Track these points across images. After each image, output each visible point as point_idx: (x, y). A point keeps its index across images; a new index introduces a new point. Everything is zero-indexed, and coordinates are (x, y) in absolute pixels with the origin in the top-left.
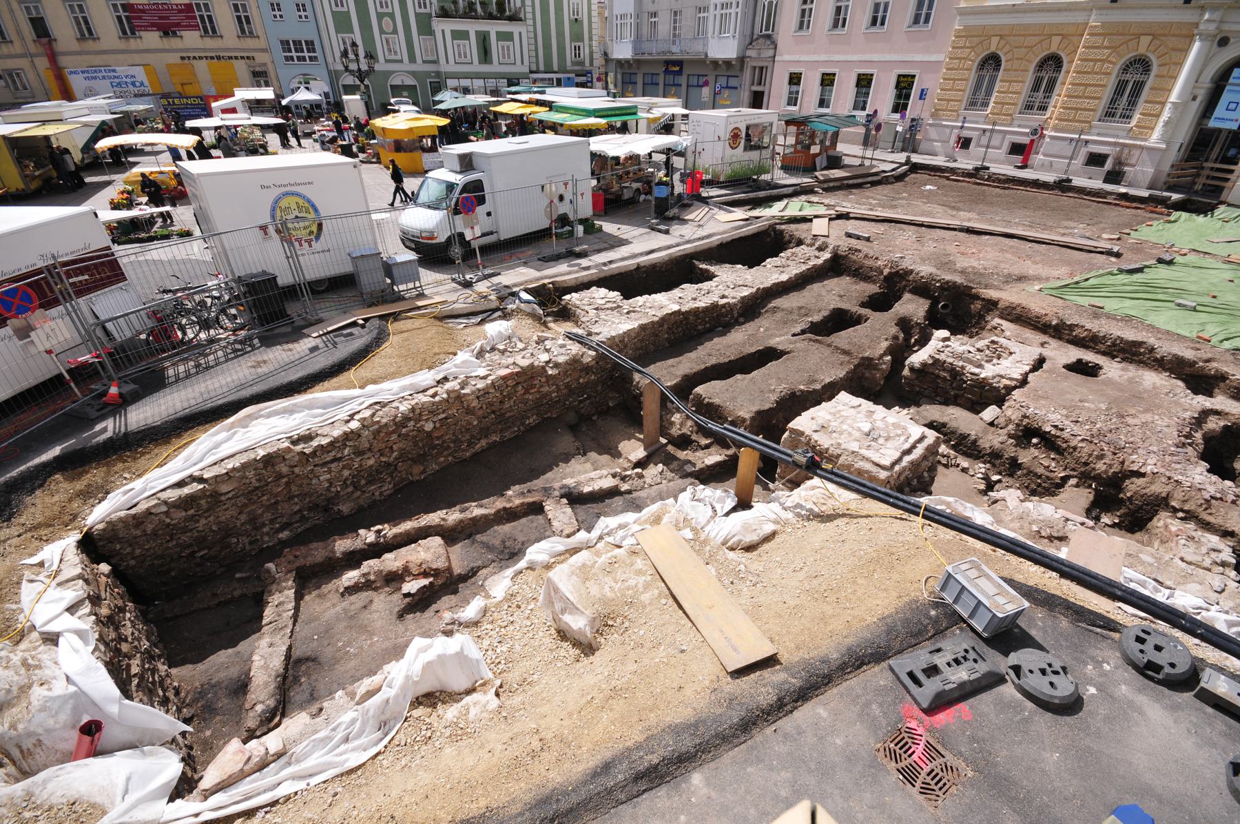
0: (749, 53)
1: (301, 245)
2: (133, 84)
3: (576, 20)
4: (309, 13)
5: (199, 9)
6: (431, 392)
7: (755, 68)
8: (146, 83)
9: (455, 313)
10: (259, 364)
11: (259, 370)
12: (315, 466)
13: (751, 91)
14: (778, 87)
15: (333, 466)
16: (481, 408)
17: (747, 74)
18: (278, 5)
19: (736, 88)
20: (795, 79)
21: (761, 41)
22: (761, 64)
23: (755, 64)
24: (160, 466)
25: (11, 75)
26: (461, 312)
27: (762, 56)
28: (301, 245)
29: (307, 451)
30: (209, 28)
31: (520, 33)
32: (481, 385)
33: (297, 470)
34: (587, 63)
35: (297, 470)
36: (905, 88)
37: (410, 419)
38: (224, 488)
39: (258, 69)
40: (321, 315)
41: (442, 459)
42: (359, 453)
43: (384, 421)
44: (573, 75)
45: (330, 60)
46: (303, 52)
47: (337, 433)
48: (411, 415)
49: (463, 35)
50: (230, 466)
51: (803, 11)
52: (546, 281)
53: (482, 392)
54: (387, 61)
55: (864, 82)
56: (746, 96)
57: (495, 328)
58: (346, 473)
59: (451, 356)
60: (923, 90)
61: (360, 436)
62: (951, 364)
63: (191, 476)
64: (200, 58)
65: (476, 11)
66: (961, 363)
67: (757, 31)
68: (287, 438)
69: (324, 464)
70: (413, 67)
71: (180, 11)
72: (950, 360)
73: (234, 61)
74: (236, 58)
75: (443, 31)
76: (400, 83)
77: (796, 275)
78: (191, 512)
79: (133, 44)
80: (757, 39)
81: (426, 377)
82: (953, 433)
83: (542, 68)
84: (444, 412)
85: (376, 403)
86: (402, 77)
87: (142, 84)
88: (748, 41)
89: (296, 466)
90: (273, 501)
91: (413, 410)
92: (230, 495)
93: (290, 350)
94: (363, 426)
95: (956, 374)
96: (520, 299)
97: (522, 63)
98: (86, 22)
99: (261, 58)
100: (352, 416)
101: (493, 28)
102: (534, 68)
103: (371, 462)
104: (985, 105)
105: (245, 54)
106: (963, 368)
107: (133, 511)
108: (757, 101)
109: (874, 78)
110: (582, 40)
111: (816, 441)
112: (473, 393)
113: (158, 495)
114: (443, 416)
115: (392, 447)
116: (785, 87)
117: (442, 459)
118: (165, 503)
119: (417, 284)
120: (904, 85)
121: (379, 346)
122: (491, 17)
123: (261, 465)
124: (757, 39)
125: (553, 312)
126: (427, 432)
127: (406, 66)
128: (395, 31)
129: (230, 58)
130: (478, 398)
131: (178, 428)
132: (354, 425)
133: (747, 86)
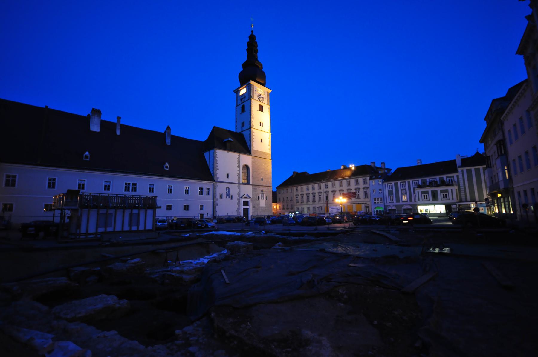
4: (382, 191)
18: (375, 190)
25: (320, 208)
30: (358, 197)
39: (367, 206)
45: (385, 203)
46: (376, 201)
54: (389, 203)
64: (355, 204)
70: (411, 203)
71: (353, 193)
73: (362, 204)
74: (362, 203)
76: (406, 208)
86: (407, 206)
99: (368, 203)
105: (364, 202)
127: (409, 203)
129: (361, 203)
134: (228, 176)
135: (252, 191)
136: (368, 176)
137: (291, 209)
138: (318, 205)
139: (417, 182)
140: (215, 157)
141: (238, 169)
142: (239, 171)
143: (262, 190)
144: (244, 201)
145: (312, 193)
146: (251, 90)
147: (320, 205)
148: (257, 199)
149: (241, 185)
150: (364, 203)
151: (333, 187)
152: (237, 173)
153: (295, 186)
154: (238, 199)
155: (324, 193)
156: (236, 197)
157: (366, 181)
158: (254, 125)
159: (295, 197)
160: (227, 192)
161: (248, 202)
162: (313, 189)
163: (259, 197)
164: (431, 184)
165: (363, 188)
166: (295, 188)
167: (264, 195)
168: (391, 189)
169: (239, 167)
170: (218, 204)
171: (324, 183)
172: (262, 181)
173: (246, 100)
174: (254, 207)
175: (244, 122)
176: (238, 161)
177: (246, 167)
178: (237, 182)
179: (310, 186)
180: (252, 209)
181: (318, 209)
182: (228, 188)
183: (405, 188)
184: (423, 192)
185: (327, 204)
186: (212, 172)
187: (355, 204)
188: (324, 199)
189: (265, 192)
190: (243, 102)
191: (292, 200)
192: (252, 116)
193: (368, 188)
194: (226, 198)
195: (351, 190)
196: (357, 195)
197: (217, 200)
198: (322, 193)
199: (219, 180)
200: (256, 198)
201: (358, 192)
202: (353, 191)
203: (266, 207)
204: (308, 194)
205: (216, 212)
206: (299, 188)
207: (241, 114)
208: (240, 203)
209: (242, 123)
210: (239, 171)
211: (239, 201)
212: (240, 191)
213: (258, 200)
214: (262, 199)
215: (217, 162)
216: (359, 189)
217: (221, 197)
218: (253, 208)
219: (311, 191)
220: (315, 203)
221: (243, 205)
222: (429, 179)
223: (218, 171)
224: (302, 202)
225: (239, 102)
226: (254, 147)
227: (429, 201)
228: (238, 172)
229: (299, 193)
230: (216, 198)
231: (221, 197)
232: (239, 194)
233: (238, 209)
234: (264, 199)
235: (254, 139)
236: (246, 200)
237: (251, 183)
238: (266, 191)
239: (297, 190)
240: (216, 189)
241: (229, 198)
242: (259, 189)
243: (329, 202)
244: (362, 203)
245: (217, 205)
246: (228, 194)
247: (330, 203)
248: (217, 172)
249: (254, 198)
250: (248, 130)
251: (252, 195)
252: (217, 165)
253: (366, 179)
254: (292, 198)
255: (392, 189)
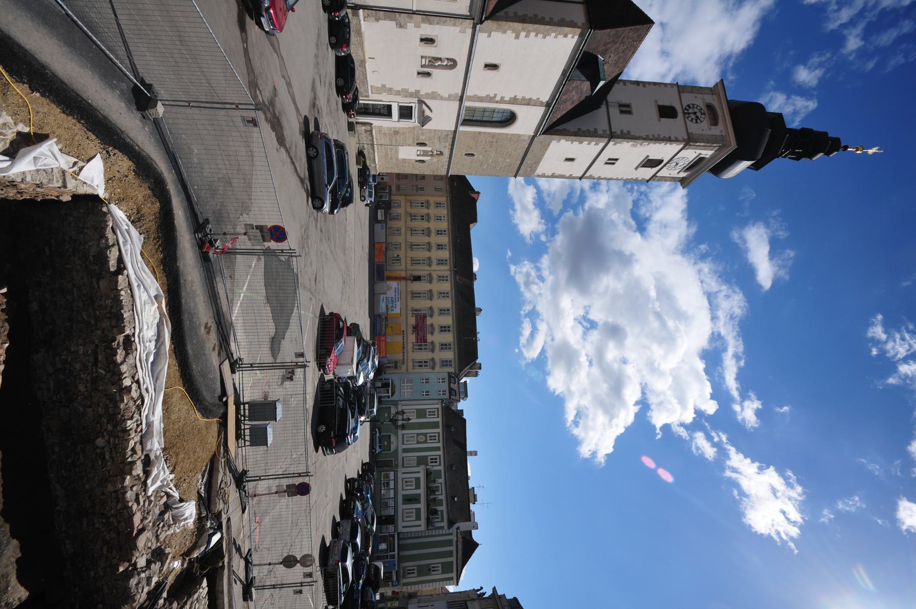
1: (289, 373)
2: (392, 307)
3: (430, 570)
5: (424, 345)
6: (138, 448)
8: (393, 312)
9: (215, 473)
10: (208, 329)
11: (203, 328)
12: (97, 346)
15: (91, 359)
16: (103, 494)
24: (142, 253)
26: (214, 477)
28: (289, 373)
29: (115, 344)
31: (420, 526)
32: (130, 495)
33: (99, 332)
34: (405, 581)
35: (99, 332)
37: (115, 427)
38: (103, 284)
39: (399, 364)
40: (237, 374)
41: (57, 449)
42: (95, 381)
43: (122, 406)
44: (397, 569)
45: (403, 403)
47: (124, 368)
48: (119, 428)
49: (418, 487)
50: (123, 293)
52: (226, 560)
53: (120, 496)
57: (190, 510)
58: (78, 366)
59: (171, 468)
61: (113, 384)
63: (125, 268)
64: (403, 339)
65: (431, 495)
68: (134, 335)
69: (95, 353)
71: (424, 337)
73: (402, 354)
74: (404, 356)
75: (419, 472)
76: (392, 441)
78: (91, 258)
79: (410, 312)
81: (156, 445)
83: (402, 542)
84: (111, 457)
85: (143, 402)
86: (395, 443)
87: (392, 310)
89: (103, 332)
90: (75, 309)
91: (126, 432)
92: (95, 284)
93: (214, 349)
94: (123, 389)
96: (214, 534)
97: (404, 527)
98: (419, 297)
99: (404, 367)
100: (138, 382)
101: (422, 506)
102: (401, 536)
103: (81, 388)
105: (405, 360)
107: (109, 230)
110: (419, 575)
112: (124, 488)
113: (116, 247)
114: (107, 456)
115: (90, 407)
117: (57, 449)
118: (108, 247)
119: (247, 444)
121: (199, 410)
122: (428, 505)
123: (114, 310)
125: (193, 567)
126: (95, 440)
127: (401, 447)
128: (418, 442)
129: (404, 353)
130: (116, 492)
131: (170, 273)
132: (127, 382)
134: (493, 67)
135: (442, 131)
136: (455, 370)
137: (399, 185)
138: (404, 256)
139: (438, 464)
140: (559, 29)
141: (507, 99)
142: (502, 101)
143: (441, 153)
144: (412, 107)
145: (432, 242)
146: (710, 145)
147: (403, 261)
148: (418, 139)
149: (458, 103)
150: (404, 359)
151: (440, 293)
152: (495, 95)
153: (447, 199)
154: (417, 92)
155: (428, 272)
156: (424, 86)
157: (447, 365)
158: (618, 145)
159: (423, 199)
160: (440, 59)
161: (411, 118)
162: (440, 247)
163: (424, 144)
164: (430, 491)
165: (433, 359)
166: (443, 199)
167: (430, 158)
168: (428, 414)
169: (514, 101)
170: (401, 26)
171: (449, 272)
172: (466, 154)
173: (688, 122)
174: (396, 132)
175: (630, 112)
176: (530, 99)
177: (510, 119)
178: (470, 92)
179: (445, 240)
180: (391, 128)
181: (396, 256)
182: (452, 65)
183: (429, 441)
184: (418, 480)
185: (405, 279)
186: (511, 10)
187: (403, 339)
188: (415, 270)
189: (435, 159)
190: (684, 114)
191: (418, 189)
192: (640, 141)
193: (433, 368)
194: (422, 57)
195: (432, 333)
196: (421, 345)
197: (417, 26)
198: (428, 268)
199: (481, 37)
200: (422, 139)
201: (426, 349)
202: (430, 338)
203: (397, 159)
204: (429, 246)
205: (377, 20)
206: (444, 212)
207: (656, 101)
208: (406, 96)
209: (628, 106)
210: (502, 101)
211: (411, 95)
212: (442, 98)
213: (416, 142)
214: (419, 153)
215: (540, 36)
216: (433, 351)
217: (428, 41)
218: (393, 130)
219: (435, 239)
220: (409, 250)
221: (400, 104)
222: (441, 483)
223: (510, 35)
224: (411, 216)
225: (688, 99)
226: (559, 142)
227: (403, 479)
228: (498, 98)
229: (432, 211)
230: (423, 21)
231: (428, 41)
232: (434, 96)
233: (390, 91)
234: (418, 155)
235: (581, 143)
236: (415, 113)
237: (462, 129)
238: (438, 161)
239: (438, 205)
240: (454, 25)
241: (422, 66)
242: (445, 147)
243: (409, 282)
244: (404, 356)
245: (401, 26)
246: (434, 62)
247: (406, 283)
248: (509, 32)
249: (422, 134)
250: (607, 128)
251: (430, 130)
252: (533, 34)
253: (450, 365)
254: (422, 189)
255: (428, 416)
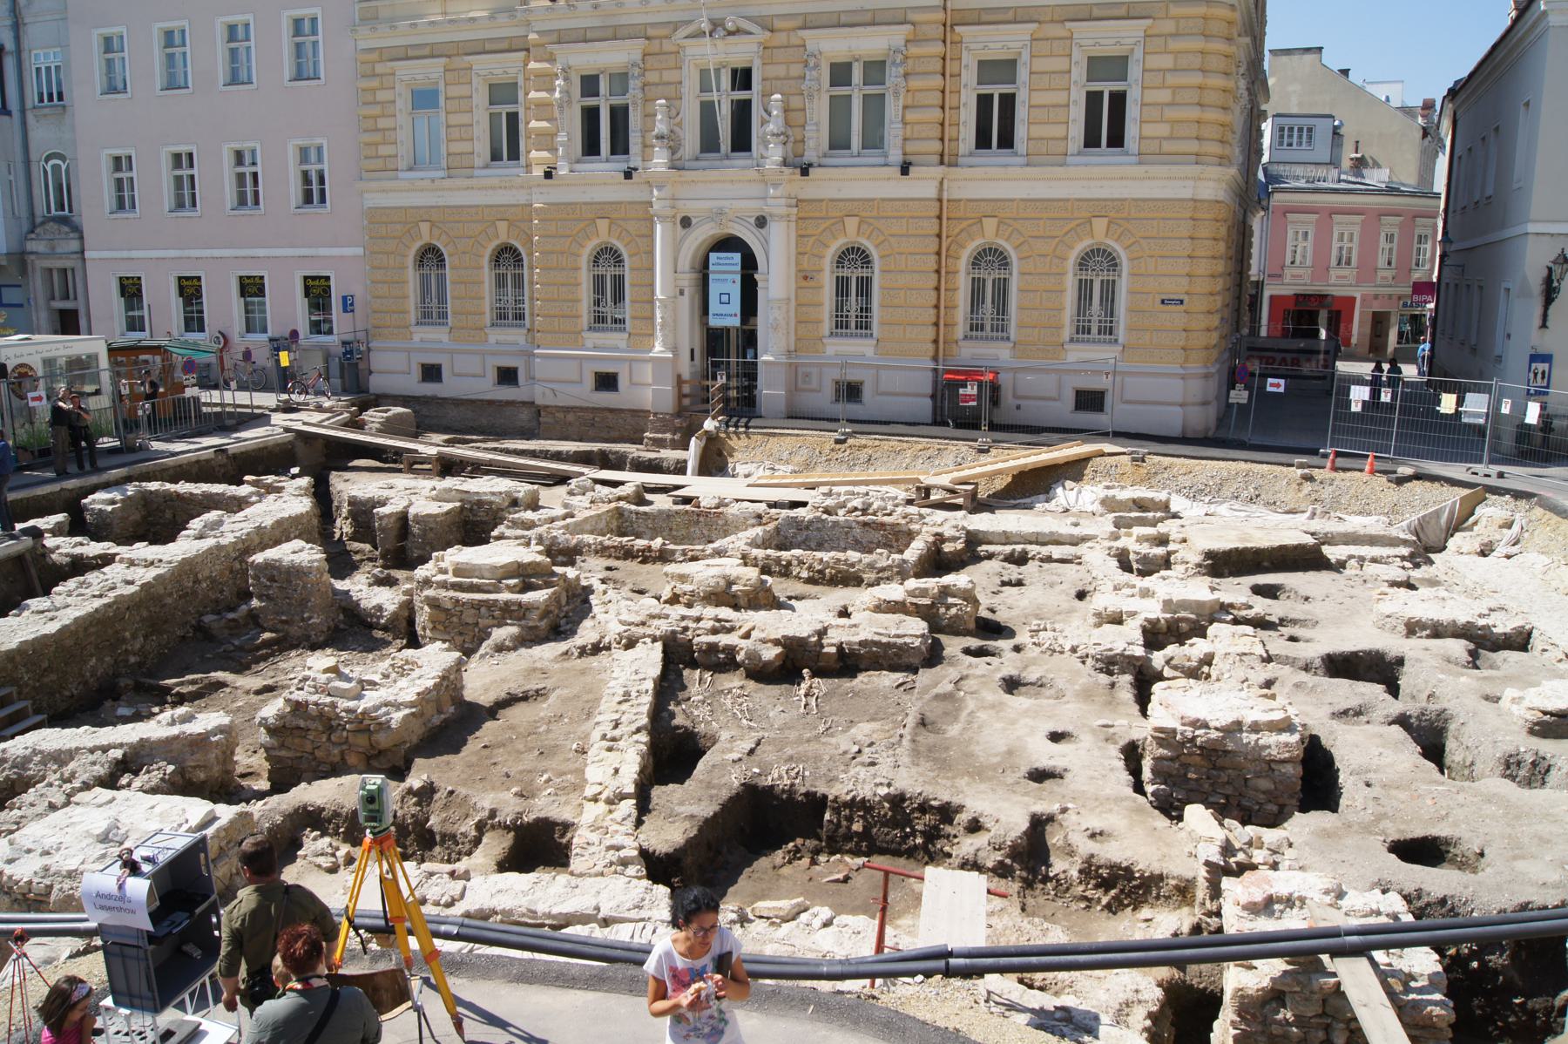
0: (31, 246)
7: (50, 270)
13: (51, 310)
14: (104, 302)
17: (37, 283)
19: (21, 306)
20: (131, 290)
21: (51, 226)
22: (60, 264)
23: (48, 264)
27: (59, 250)
36: (319, 296)
51: (119, 182)
55: (251, 288)
56: (43, 317)
60: (345, 298)
62: (316, 704)
66: (328, 700)
67: (40, 209)
72: (315, 698)
77: (76, 619)
80: (43, 223)
82: (336, 814)
88: (26, 227)
95: (327, 721)
104: (443, 315)
106: (333, 705)
108: (68, 323)
109: (266, 281)
111: (10, 877)
116: (117, 303)
120: (317, 291)
124: (43, 223)
133: (41, 301)
